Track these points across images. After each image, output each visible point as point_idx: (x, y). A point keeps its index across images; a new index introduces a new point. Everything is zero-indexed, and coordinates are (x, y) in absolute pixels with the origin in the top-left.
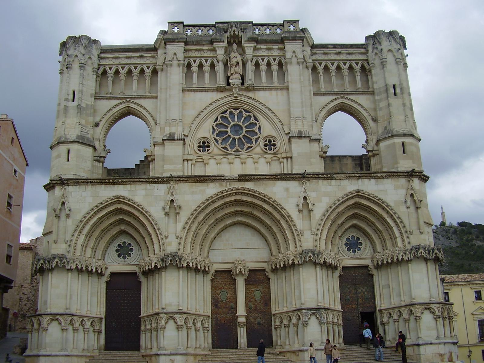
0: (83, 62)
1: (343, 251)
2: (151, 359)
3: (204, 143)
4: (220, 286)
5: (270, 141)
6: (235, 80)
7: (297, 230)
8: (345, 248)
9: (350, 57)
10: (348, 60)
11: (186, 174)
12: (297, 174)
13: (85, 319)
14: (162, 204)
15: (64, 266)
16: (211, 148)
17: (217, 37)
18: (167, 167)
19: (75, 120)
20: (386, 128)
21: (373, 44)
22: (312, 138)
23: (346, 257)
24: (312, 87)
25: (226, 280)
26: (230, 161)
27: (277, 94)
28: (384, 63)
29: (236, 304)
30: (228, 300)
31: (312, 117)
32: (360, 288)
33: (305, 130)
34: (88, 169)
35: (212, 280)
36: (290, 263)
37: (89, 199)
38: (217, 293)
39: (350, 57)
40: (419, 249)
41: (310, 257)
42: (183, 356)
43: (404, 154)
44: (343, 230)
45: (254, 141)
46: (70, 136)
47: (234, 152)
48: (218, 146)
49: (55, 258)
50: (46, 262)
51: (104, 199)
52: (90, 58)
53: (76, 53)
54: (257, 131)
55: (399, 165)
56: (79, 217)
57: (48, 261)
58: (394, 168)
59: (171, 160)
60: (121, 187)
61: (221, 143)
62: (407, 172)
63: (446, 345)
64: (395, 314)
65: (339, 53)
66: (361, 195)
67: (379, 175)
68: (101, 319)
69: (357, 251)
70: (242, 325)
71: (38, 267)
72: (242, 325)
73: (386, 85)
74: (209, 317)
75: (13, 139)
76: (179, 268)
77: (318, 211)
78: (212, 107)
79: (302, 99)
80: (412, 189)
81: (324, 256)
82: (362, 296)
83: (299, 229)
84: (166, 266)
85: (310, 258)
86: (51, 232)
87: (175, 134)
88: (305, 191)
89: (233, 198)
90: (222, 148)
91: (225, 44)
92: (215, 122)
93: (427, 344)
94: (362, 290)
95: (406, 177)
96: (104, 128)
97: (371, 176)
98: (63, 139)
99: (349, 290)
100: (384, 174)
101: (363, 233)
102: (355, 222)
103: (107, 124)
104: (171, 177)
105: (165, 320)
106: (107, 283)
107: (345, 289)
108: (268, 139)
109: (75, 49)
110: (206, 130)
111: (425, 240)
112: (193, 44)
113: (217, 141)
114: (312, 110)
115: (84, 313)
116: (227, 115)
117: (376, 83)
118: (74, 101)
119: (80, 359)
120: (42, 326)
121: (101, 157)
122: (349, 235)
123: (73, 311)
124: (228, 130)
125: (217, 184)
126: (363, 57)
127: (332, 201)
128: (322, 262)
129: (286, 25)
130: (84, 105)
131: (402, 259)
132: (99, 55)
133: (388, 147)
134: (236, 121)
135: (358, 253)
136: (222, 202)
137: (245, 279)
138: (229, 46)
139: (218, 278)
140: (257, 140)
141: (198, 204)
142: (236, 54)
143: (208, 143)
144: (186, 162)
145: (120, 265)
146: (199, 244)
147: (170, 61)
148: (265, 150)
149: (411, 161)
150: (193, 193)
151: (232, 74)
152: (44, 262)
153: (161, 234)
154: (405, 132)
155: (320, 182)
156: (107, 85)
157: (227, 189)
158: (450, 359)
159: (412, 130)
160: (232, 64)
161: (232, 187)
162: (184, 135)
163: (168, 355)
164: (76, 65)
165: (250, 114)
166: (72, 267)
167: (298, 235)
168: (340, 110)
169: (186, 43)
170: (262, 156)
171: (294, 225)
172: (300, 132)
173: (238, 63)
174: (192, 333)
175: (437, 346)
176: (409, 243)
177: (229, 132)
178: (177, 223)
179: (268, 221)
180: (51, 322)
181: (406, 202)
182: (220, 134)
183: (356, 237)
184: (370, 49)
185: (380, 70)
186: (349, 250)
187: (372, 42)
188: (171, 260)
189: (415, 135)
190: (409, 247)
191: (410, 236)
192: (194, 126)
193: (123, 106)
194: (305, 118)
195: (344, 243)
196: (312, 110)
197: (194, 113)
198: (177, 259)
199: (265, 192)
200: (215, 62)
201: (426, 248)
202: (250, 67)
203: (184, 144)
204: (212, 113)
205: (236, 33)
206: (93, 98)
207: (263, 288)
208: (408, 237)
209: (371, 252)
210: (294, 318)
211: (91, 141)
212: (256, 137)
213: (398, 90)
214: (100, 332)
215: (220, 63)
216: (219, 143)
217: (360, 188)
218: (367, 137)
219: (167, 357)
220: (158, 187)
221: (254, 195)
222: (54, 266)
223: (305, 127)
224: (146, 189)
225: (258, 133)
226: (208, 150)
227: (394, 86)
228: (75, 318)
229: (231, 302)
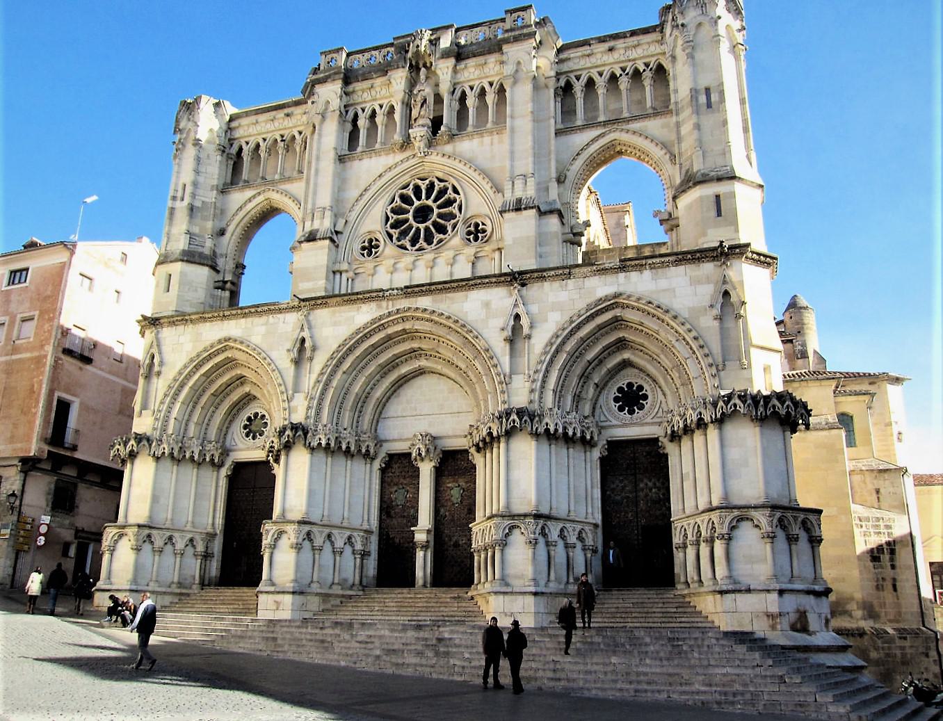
1: (609, 410)
3: (371, 241)
4: (396, 480)
5: (477, 225)
8: (614, 406)
9: (633, 54)
10: (630, 61)
13: (176, 535)
14: (289, 345)
16: (381, 249)
19: (184, 227)
20: (687, 172)
21: (673, 19)
23: (615, 422)
25: (406, 469)
27: (492, 144)
29: (417, 511)
32: (642, 481)
33: (528, 196)
34: (200, 301)
35: (383, 471)
39: (633, 54)
42: (297, 597)
43: (719, 214)
47: (416, 250)
51: (208, 344)
54: (456, 211)
60: (233, 323)
62: (715, 249)
63: (787, 596)
65: (611, 50)
67: (658, 260)
69: (637, 411)
70: (425, 547)
72: (425, 547)
77: (540, 340)
78: (384, 180)
82: (647, 495)
85: (514, 422)
88: (516, 305)
89: (399, 328)
93: (740, 591)
94: (646, 483)
95: (714, 259)
96: (234, 237)
99: (621, 485)
100: (667, 259)
102: (626, 355)
103: (239, 230)
105: (274, 533)
107: (613, 483)
108: (473, 222)
113: (390, 236)
117: (676, 91)
118: (182, 199)
119: (159, 597)
124: (410, 216)
125: (373, 305)
130: (198, 204)
131: (701, 420)
134: (423, 197)
135: (639, 414)
136: (381, 335)
139: (396, 466)
140: (454, 227)
141: (340, 342)
144: (338, 276)
146: (349, 408)
149: (733, 228)
150: (335, 324)
154: (719, 173)
155: (547, 284)
162: (337, 233)
163: (272, 593)
175: (763, 595)
181: (712, 306)
184: (668, 30)
186: (621, 409)
188: (289, 436)
192: (354, 215)
193: (260, 198)
198: (300, 433)
203: (337, 247)
204: (384, 190)
206: (215, 192)
207: (467, 482)
213: (714, 97)
216: (394, 238)
217: (621, 289)
219: (271, 596)
223: (528, 193)
224: (266, 323)
225: (458, 214)
226: (376, 253)
227: (708, 91)
228: (154, 532)
229: (413, 507)
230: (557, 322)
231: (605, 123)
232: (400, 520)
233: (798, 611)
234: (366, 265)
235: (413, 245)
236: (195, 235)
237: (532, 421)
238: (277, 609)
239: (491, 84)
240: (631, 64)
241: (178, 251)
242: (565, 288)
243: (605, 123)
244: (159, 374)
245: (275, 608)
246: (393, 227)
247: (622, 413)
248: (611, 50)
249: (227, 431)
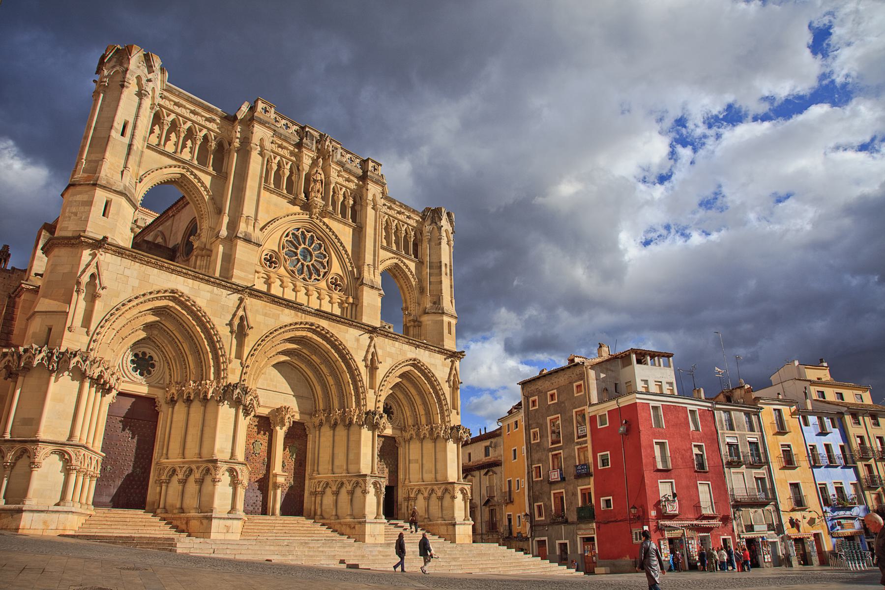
2: (187, 523)
12: (368, 326)
37: (136, 283)
49: (75, 356)
53: (139, 73)
56: (115, 302)
109: (139, 67)
112: (280, 138)
116: (299, 233)
118: (123, 134)
133: (436, 322)
145: (133, 382)
150: (265, 315)
161: (307, 320)
169: (275, 133)
172: (372, 281)
219: (222, 521)
224: (212, 292)
242: (394, 346)
243: (394, 253)
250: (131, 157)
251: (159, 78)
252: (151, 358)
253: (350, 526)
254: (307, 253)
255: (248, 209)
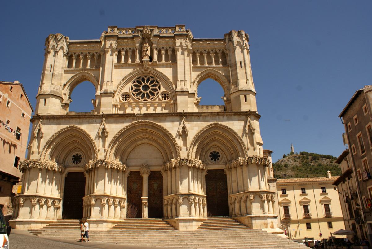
0: (58, 49)
3: (126, 96)
6: (146, 59)
7: (178, 147)
9: (216, 47)
11: (114, 113)
15: (37, 167)
17: (136, 34)
18: (102, 109)
21: (229, 38)
22: (190, 92)
24: (191, 63)
25: (137, 177)
26: (140, 106)
28: (234, 49)
29: (142, 191)
30: (138, 189)
31: (191, 81)
35: (128, 177)
36: (173, 166)
38: (131, 185)
40: (252, 158)
41: (185, 162)
43: (245, 101)
44: (208, 148)
45: (156, 94)
46: (47, 91)
48: (134, 97)
49: (31, 162)
50: (26, 164)
52: (62, 48)
54: (158, 88)
55: (242, 108)
57: (27, 164)
58: (239, 110)
59: (107, 106)
60: (74, 120)
61: (136, 96)
62: (247, 112)
64: (238, 198)
66: (217, 126)
68: (59, 200)
69: (217, 160)
71: (21, 167)
73: (236, 62)
74: (124, 199)
75: (22, 96)
76: (107, 169)
79: (184, 69)
80: (249, 122)
81: (194, 162)
83: (179, 146)
84: (98, 168)
86: (31, 146)
87: (108, 90)
88: (184, 123)
90: (136, 98)
91: (140, 40)
92: (133, 83)
97: (224, 115)
98: (42, 93)
101: (221, 149)
104: (103, 115)
106: (66, 178)
109: (53, 42)
110: (128, 88)
111: (257, 153)
113: (134, 95)
114: (191, 76)
115: (48, 195)
117: (230, 60)
118: (51, 71)
120: (20, 203)
121: (66, 104)
122: (212, 150)
123: (41, 194)
124: (141, 88)
125: (131, 119)
126: (223, 46)
127: (200, 129)
128: (192, 165)
129: (177, 29)
132: (68, 46)
134: (146, 82)
137: (148, 177)
138: (143, 40)
139: (133, 175)
140: (157, 94)
142: (148, 45)
143: (128, 95)
147: (108, 48)
148: (162, 100)
149: (250, 106)
151: (144, 56)
152: (25, 164)
153: (96, 149)
154: (246, 88)
156: (72, 64)
157: (136, 122)
158: (272, 227)
159: (250, 87)
160: (144, 51)
161: (140, 121)
162: (114, 91)
164: (52, 52)
165: (154, 79)
166: (42, 168)
167: (178, 150)
168: (209, 77)
170: (160, 104)
171: (177, 144)
172: (182, 89)
173: (147, 50)
174: (112, 207)
176: (247, 155)
177: (141, 89)
178: (106, 142)
179: (161, 142)
180: (26, 200)
182: (135, 91)
183: (216, 152)
184: (227, 41)
185: (233, 53)
186: (212, 159)
187: (227, 37)
189: (252, 90)
190: (247, 158)
191: (247, 150)
193: (80, 75)
194: (185, 80)
195: (209, 155)
196: (191, 76)
197: (122, 79)
198: (104, 163)
199: (159, 124)
200: (135, 49)
201: (257, 158)
202: (155, 52)
203: (114, 96)
205: (148, 32)
206: (63, 70)
208: (246, 152)
209: (225, 161)
210: (174, 199)
211: (60, 94)
212: (157, 92)
213: (243, 65)
214: (58, 208)
215: (138, 50)
216: (135, 95)
218: (225, 93)
220: (96, 120)
221: (153, 126)
222: (30, 166)
225: (159, 90)
226: (128, 100)
229: (140, 190)
230: (197, 131)
231: (207, 67)
232: (135, 195)
233: (271, 222)
234: (125, 104)
235: (142, 98)
236: (55, 85)
237: (190, 162)
238: (98, 227)
239: (170, 48)
240: (214, 49)
241: (50, 91)
244: (42, 137)
245: (96, 226)
246: (134, 91)
247: (212, 161)
248: (209, 43)
249: (65, 160)
250: (53, 78)
251: (65, 41)
252: (80, 155)
253: (174, 221)
254: (146, 88)
255: (106, 79)
